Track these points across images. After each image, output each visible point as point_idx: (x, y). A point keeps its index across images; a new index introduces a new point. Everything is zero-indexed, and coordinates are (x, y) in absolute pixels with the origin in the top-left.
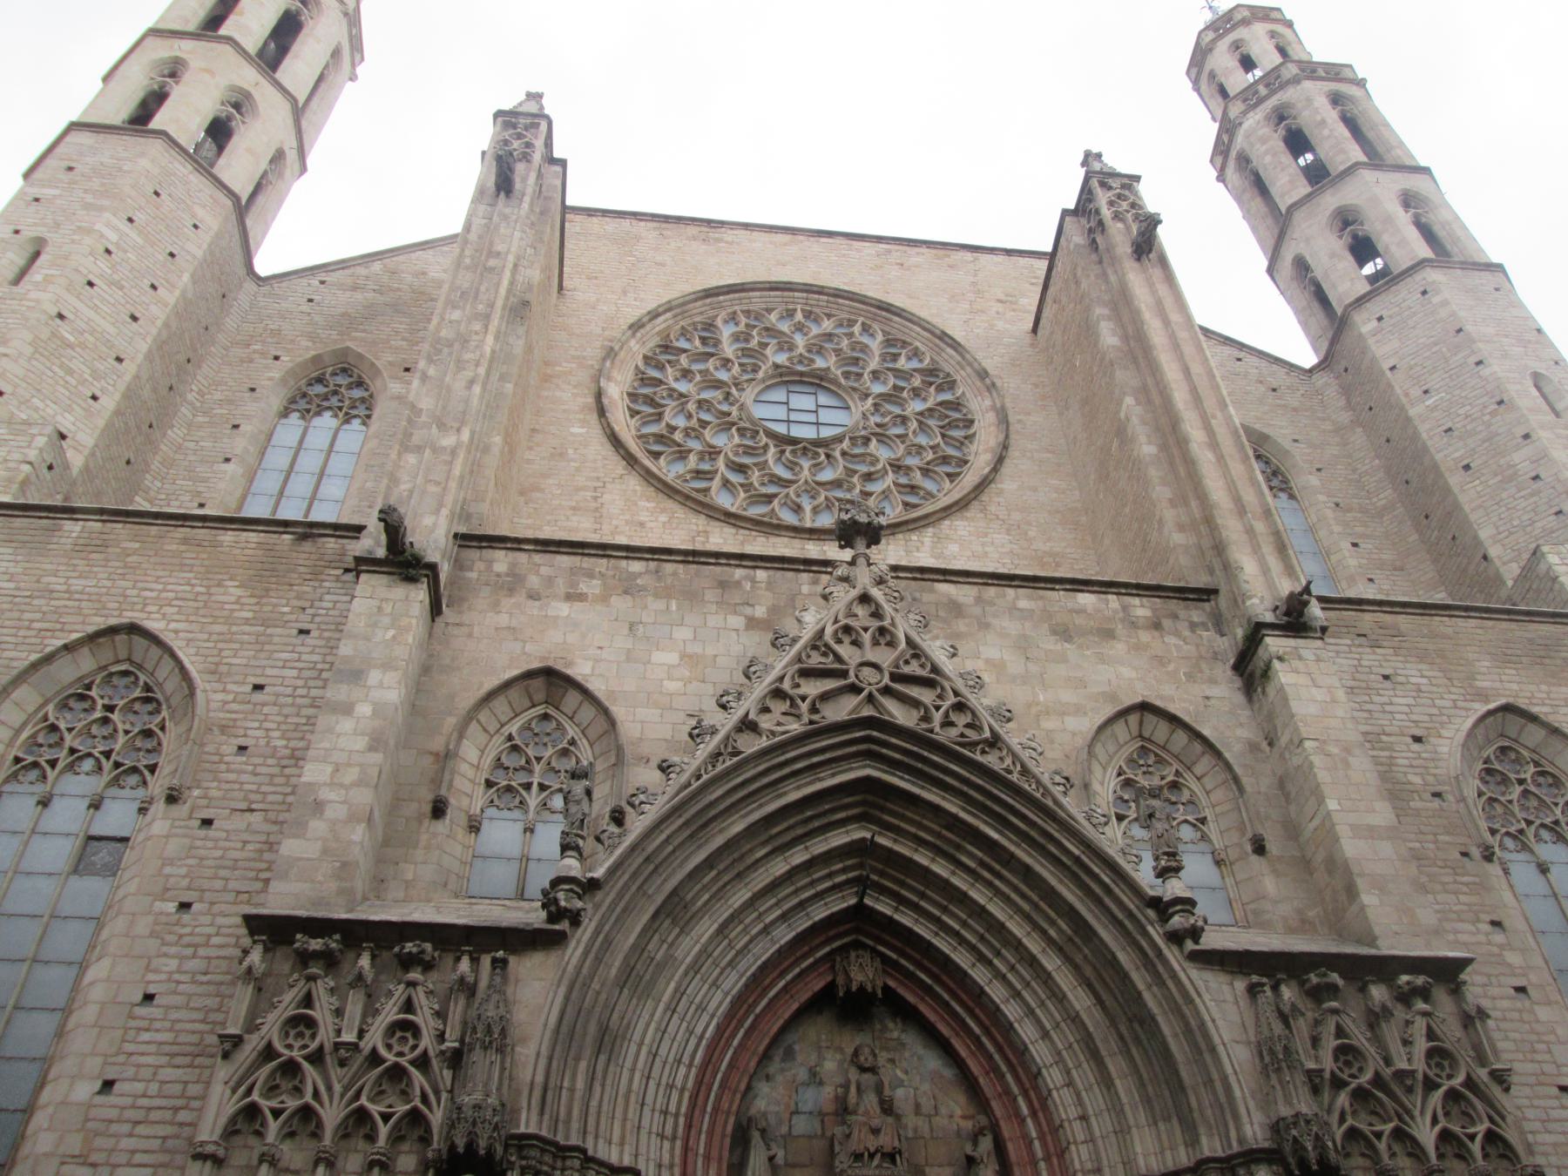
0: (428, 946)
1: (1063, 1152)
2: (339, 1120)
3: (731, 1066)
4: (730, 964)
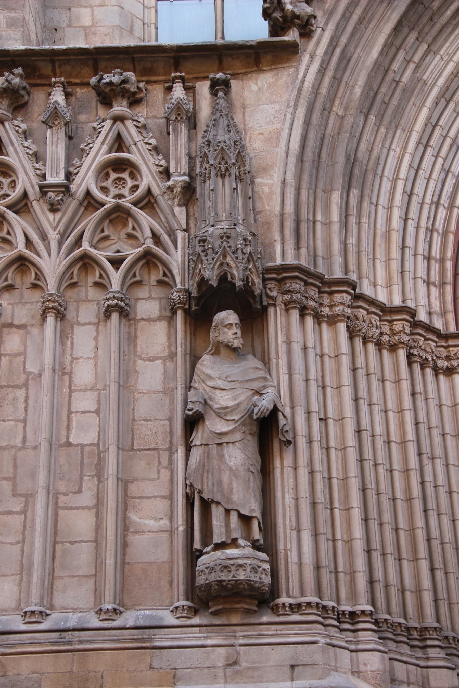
0: (130, 75)
2: (62, 268)
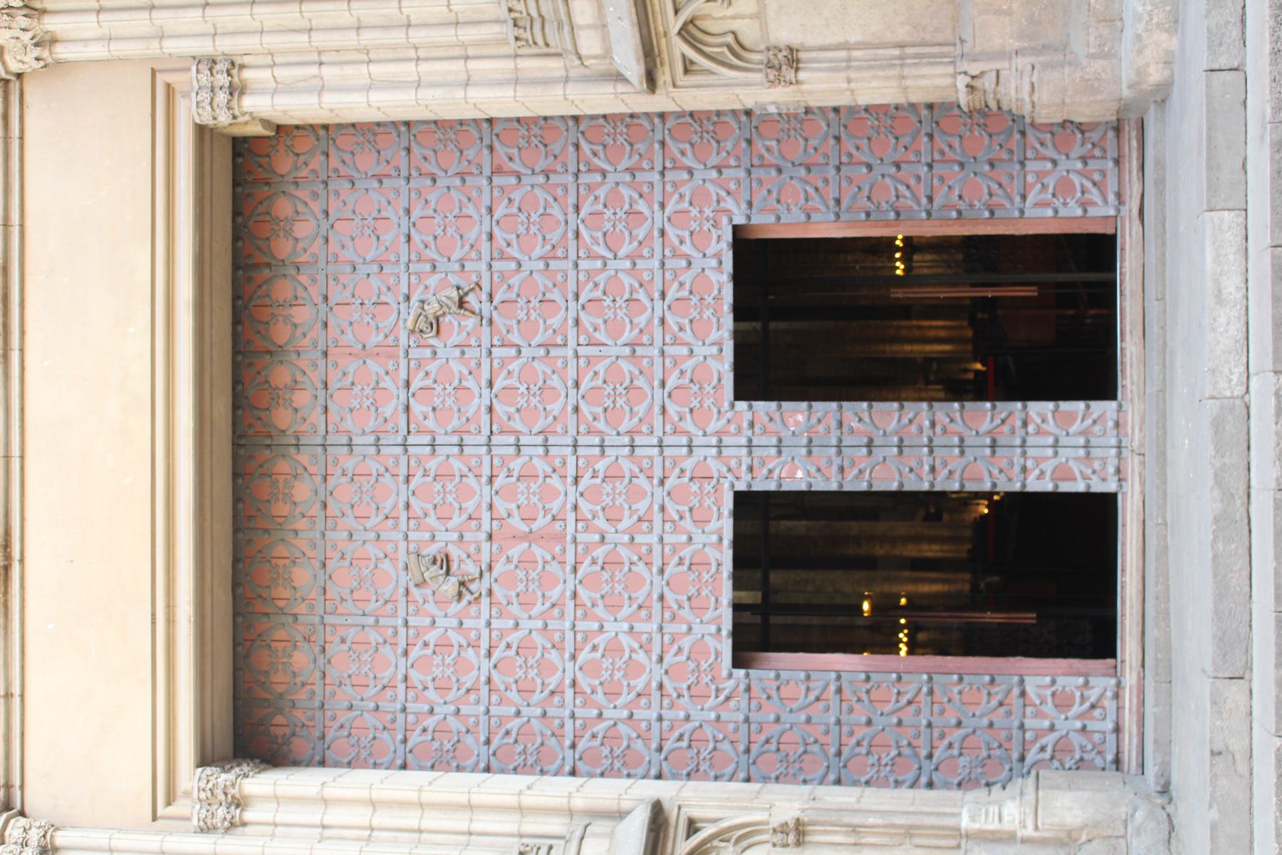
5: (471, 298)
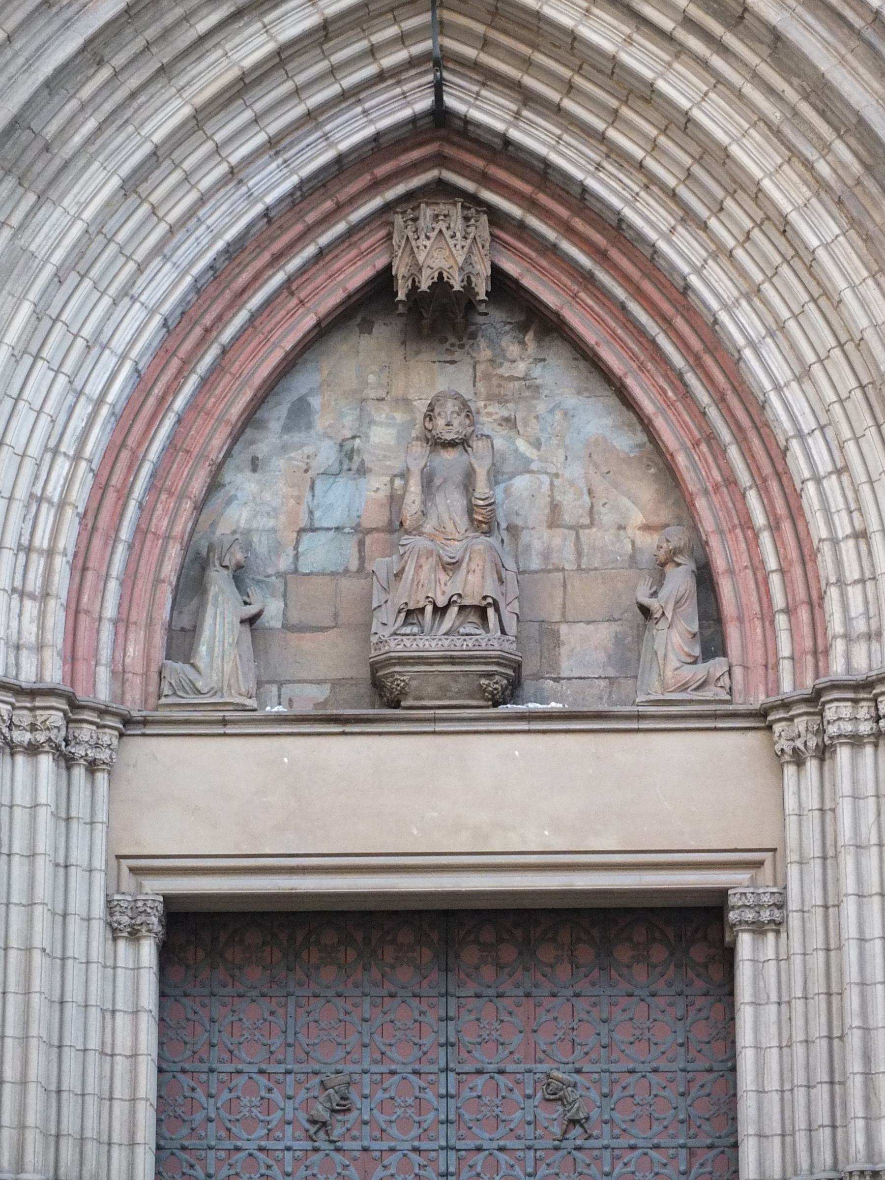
1: (821, 598)
3: (172, 446)
4: (158, 250)
5: (578, 1130)
